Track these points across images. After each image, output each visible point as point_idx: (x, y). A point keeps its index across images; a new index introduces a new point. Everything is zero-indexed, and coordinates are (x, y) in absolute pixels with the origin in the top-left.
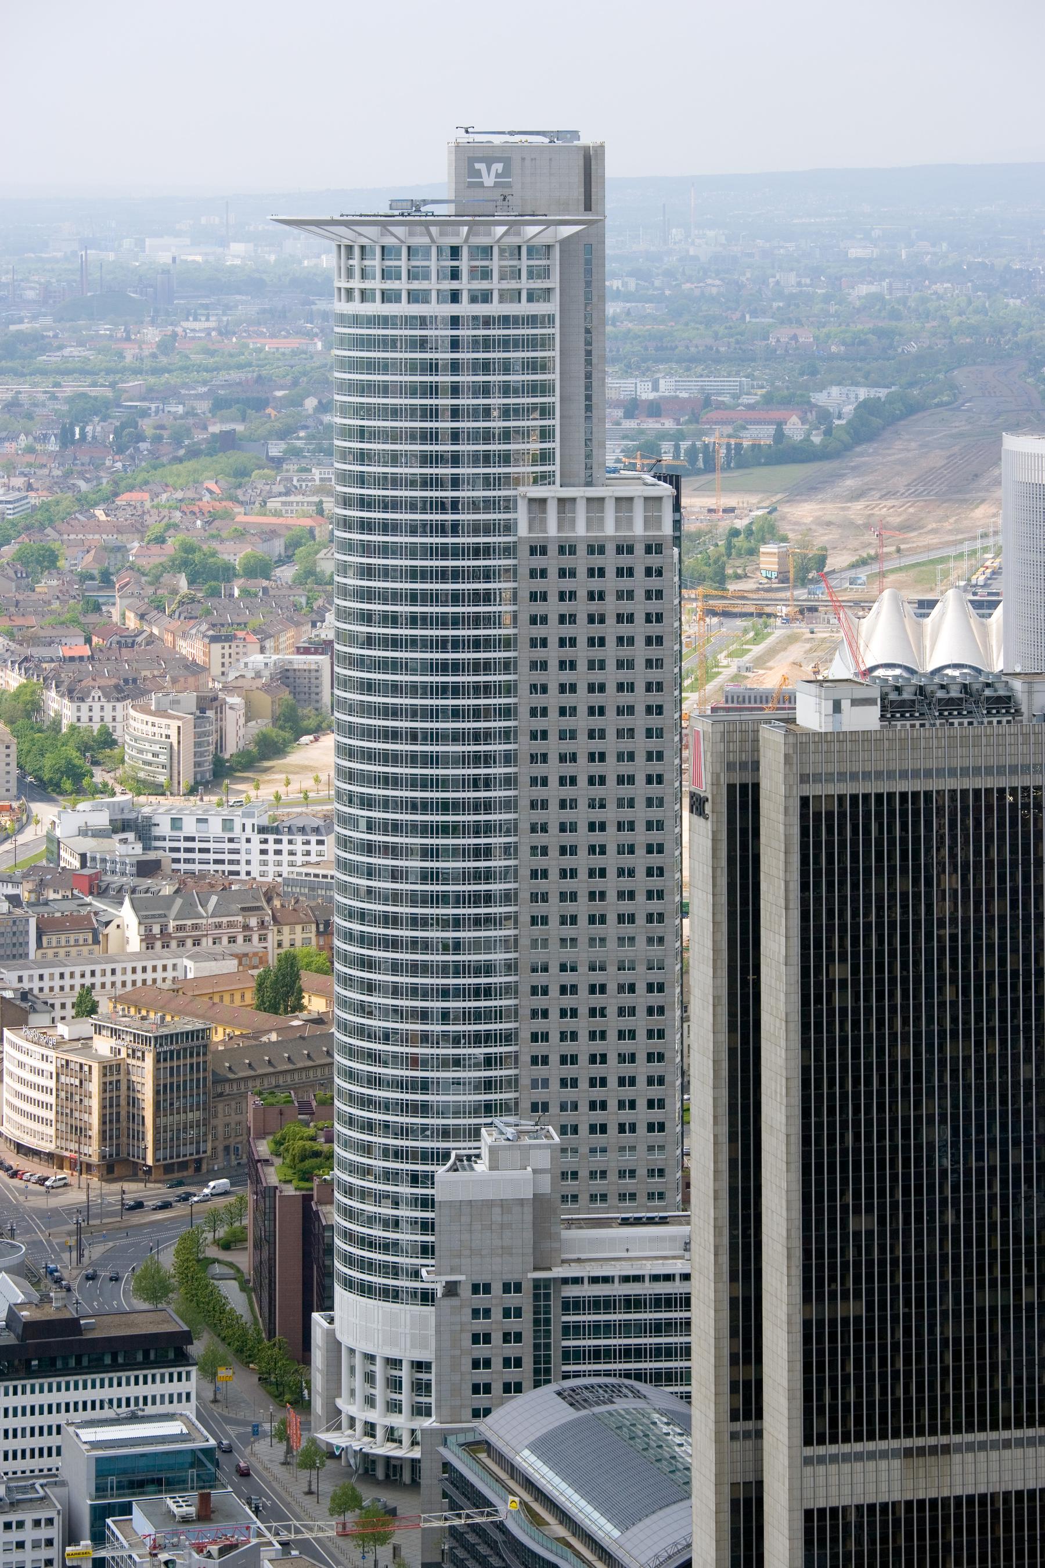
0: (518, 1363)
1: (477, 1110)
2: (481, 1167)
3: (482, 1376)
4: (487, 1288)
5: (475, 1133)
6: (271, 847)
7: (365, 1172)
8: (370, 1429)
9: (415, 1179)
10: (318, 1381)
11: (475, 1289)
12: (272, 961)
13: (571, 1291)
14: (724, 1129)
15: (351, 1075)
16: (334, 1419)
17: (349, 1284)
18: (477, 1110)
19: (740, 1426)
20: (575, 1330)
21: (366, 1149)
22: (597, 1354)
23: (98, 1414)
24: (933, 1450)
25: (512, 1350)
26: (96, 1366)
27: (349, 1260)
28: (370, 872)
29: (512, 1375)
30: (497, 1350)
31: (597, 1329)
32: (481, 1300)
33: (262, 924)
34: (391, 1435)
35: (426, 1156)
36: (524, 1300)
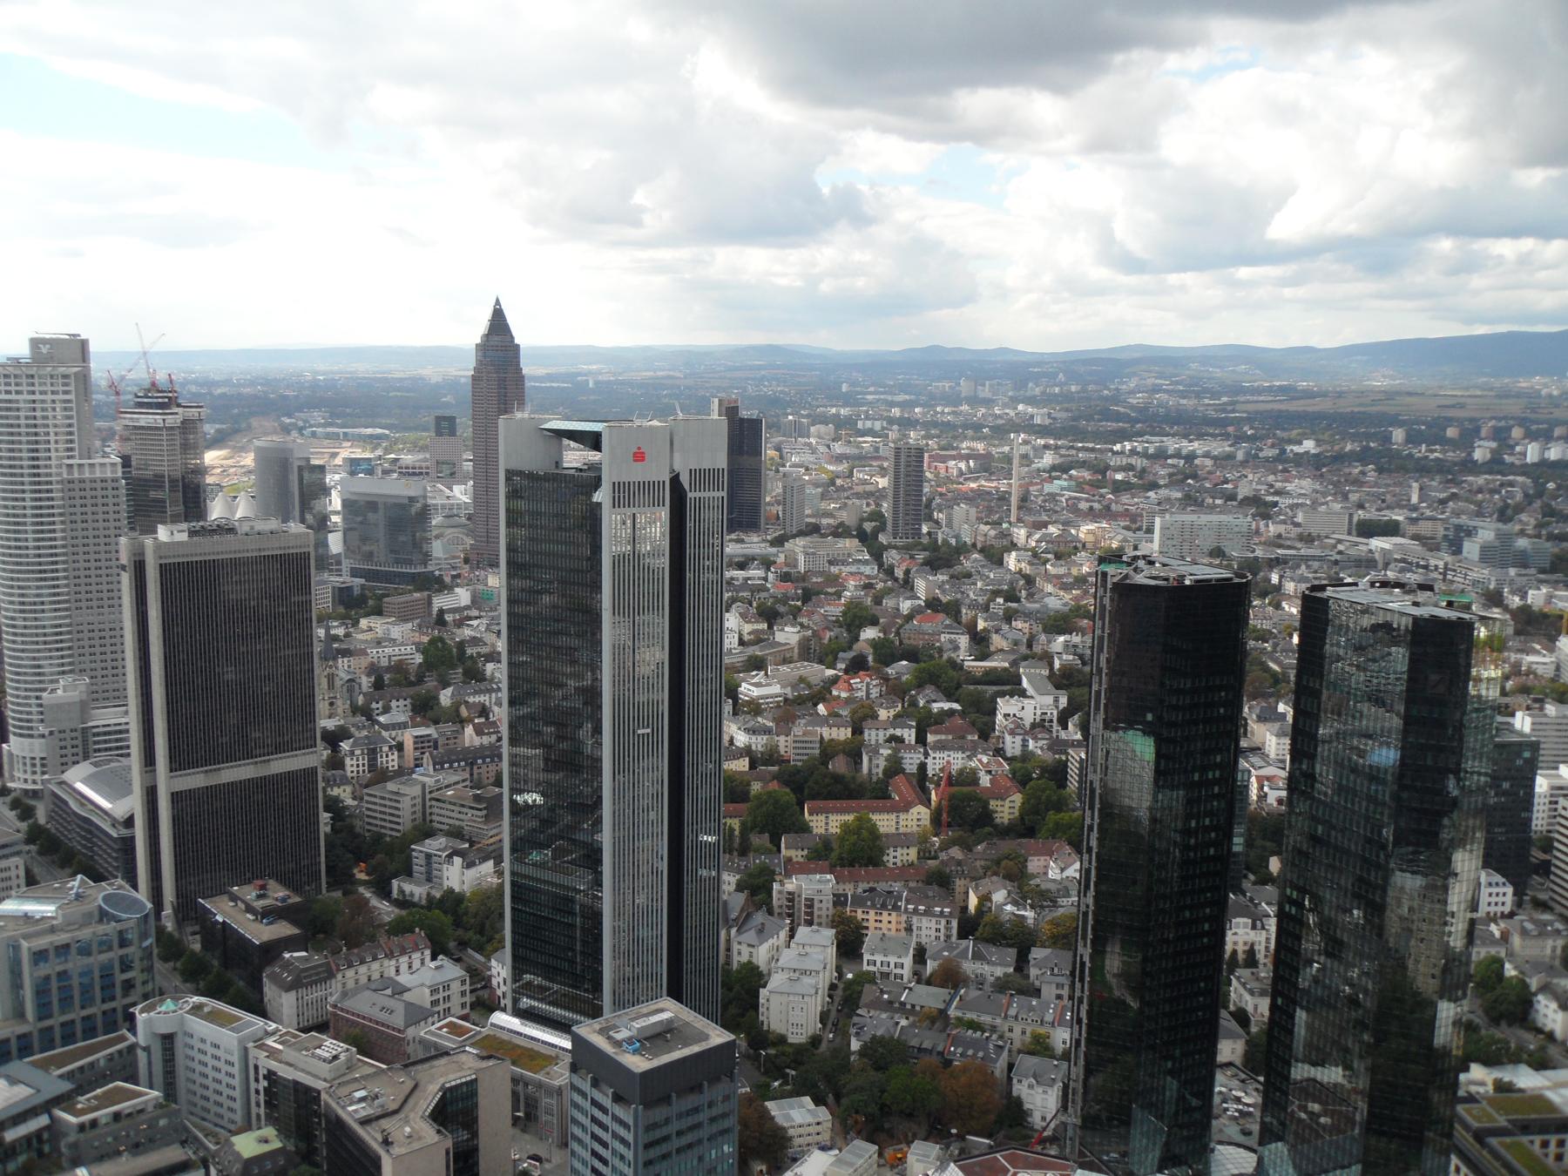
1: (59, 673)
2: (60, 692)
3: (64, 760)
5: (57, 681)
7: (18, 697)
8: (26, 781)
9: (38, 698)
10: (6, 767)
13: (95, 730)
15: (11, 665)
16: (12, 779)
17: (15, 734)
18: (59, 673)
20: (96, 743)
21: (17, 689)
22: (106, 750)
25: (75, 750)
27: (14, 726)
29: (75, 758)
30: (69, 751)
31: (105, 742)
32: (62, 736)
34: (34, 782)
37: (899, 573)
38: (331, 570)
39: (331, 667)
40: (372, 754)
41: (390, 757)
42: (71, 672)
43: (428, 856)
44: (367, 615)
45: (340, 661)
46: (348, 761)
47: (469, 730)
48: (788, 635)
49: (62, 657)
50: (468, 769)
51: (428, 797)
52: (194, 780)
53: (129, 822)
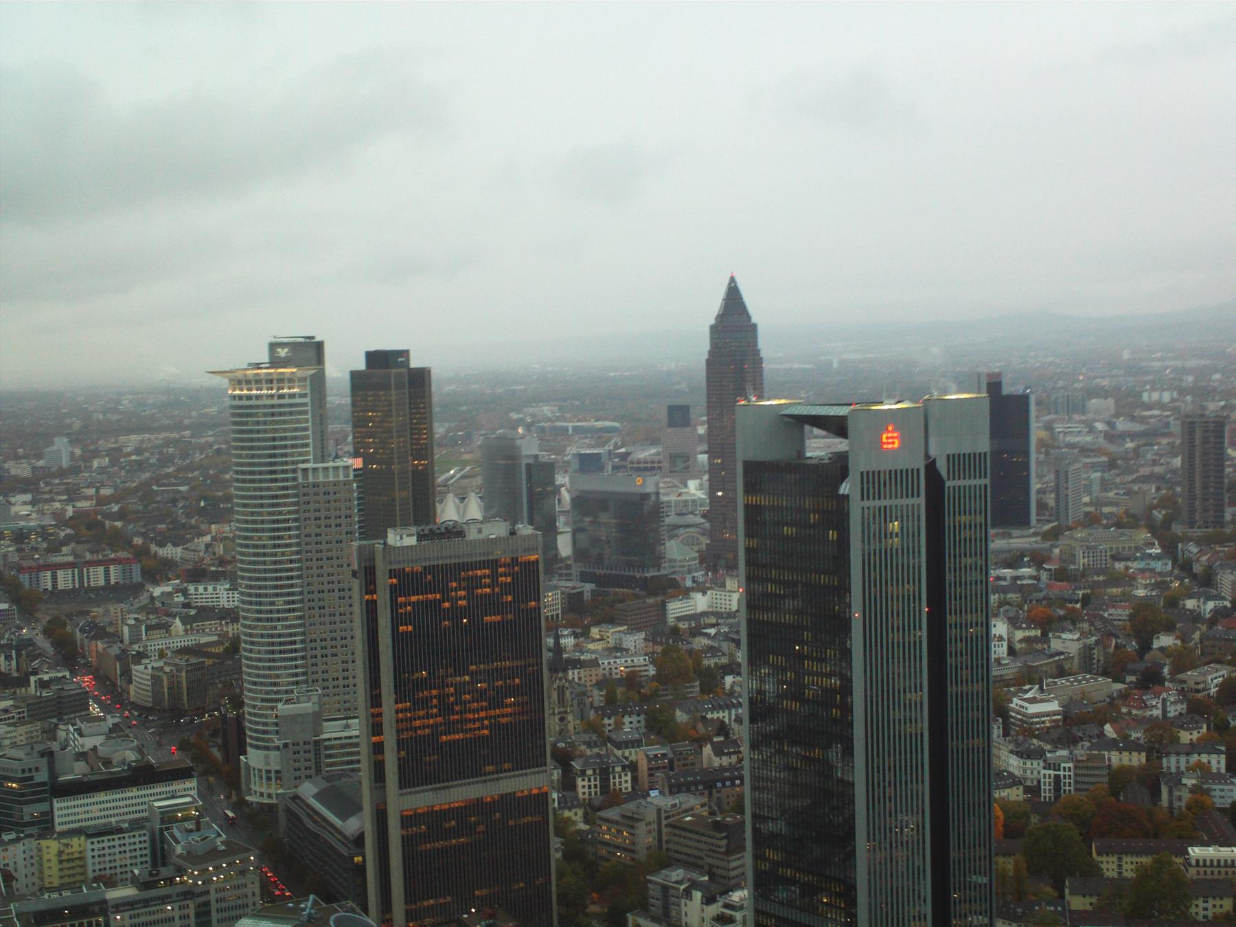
0: (310, 768)
1: (293, 683)
3: (298, 773)
4: (298, 744)
6: (231, 595)
8: (262, 795)
10: (243, 780)
11: (294, 745)
12: (231, 635)
13: (326, 743)
14: (368, 685)
17: (252, 746)
18: (293, 683)
19: (378, 785)
20: (330, 756)
23: (159, 797)
24: (444, 788)
25: (307, 764)
26: (160, 781)
28: (251, 603)
33: (227, 623)
35: (272, 700)
36: (311, 747)
37: (1197, 568)
38: (561, 575)
39: (561, 679)
40: (605, 773)
41: (624, 778)
42: (306, 681)
43: (665, 889)
44: (598, 623)
45: (570, 672)
46: (580, 782)
47: (707, 750)
48: (1068, 642)
49: (296, 667)
50: (706, 792)
51: (664, 822)
52: (424, 799)
53: (359, 840)
